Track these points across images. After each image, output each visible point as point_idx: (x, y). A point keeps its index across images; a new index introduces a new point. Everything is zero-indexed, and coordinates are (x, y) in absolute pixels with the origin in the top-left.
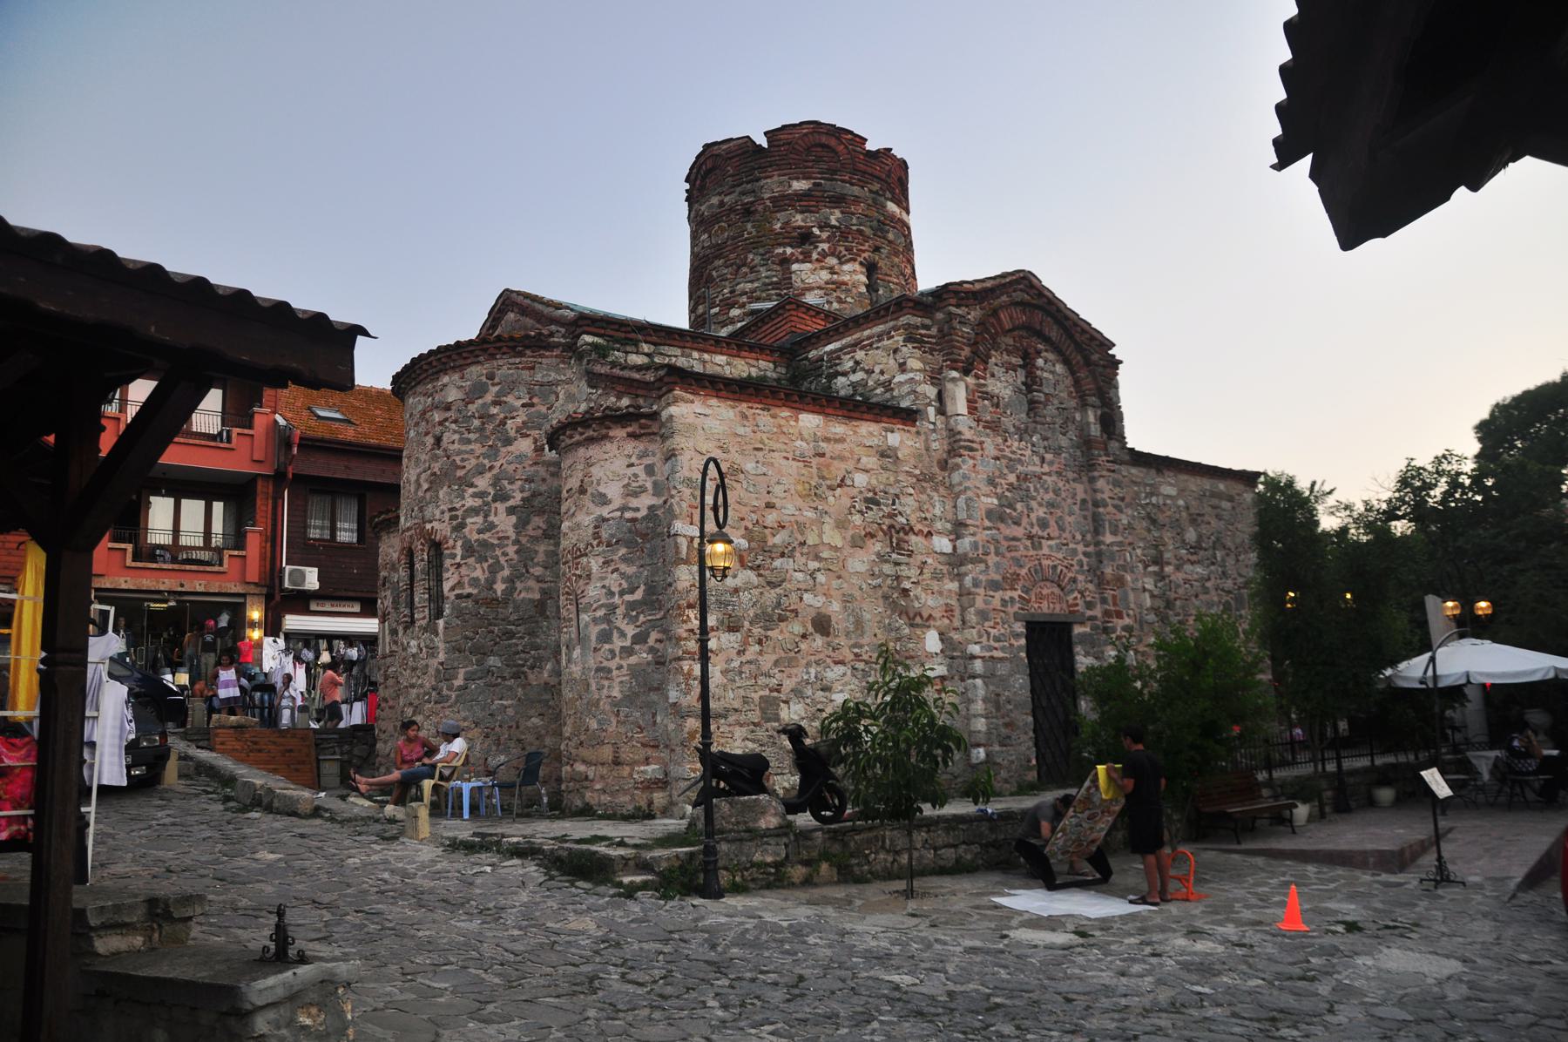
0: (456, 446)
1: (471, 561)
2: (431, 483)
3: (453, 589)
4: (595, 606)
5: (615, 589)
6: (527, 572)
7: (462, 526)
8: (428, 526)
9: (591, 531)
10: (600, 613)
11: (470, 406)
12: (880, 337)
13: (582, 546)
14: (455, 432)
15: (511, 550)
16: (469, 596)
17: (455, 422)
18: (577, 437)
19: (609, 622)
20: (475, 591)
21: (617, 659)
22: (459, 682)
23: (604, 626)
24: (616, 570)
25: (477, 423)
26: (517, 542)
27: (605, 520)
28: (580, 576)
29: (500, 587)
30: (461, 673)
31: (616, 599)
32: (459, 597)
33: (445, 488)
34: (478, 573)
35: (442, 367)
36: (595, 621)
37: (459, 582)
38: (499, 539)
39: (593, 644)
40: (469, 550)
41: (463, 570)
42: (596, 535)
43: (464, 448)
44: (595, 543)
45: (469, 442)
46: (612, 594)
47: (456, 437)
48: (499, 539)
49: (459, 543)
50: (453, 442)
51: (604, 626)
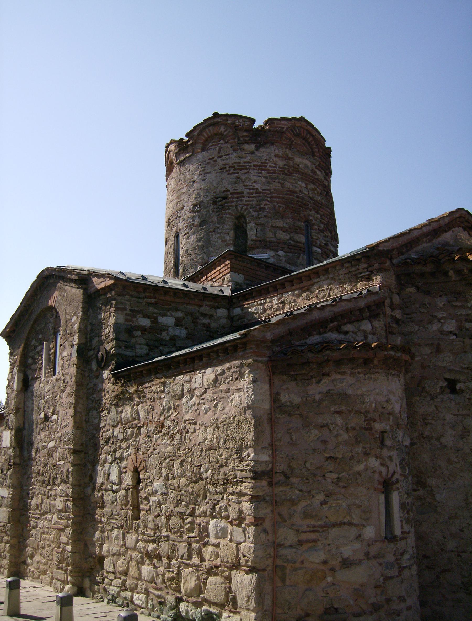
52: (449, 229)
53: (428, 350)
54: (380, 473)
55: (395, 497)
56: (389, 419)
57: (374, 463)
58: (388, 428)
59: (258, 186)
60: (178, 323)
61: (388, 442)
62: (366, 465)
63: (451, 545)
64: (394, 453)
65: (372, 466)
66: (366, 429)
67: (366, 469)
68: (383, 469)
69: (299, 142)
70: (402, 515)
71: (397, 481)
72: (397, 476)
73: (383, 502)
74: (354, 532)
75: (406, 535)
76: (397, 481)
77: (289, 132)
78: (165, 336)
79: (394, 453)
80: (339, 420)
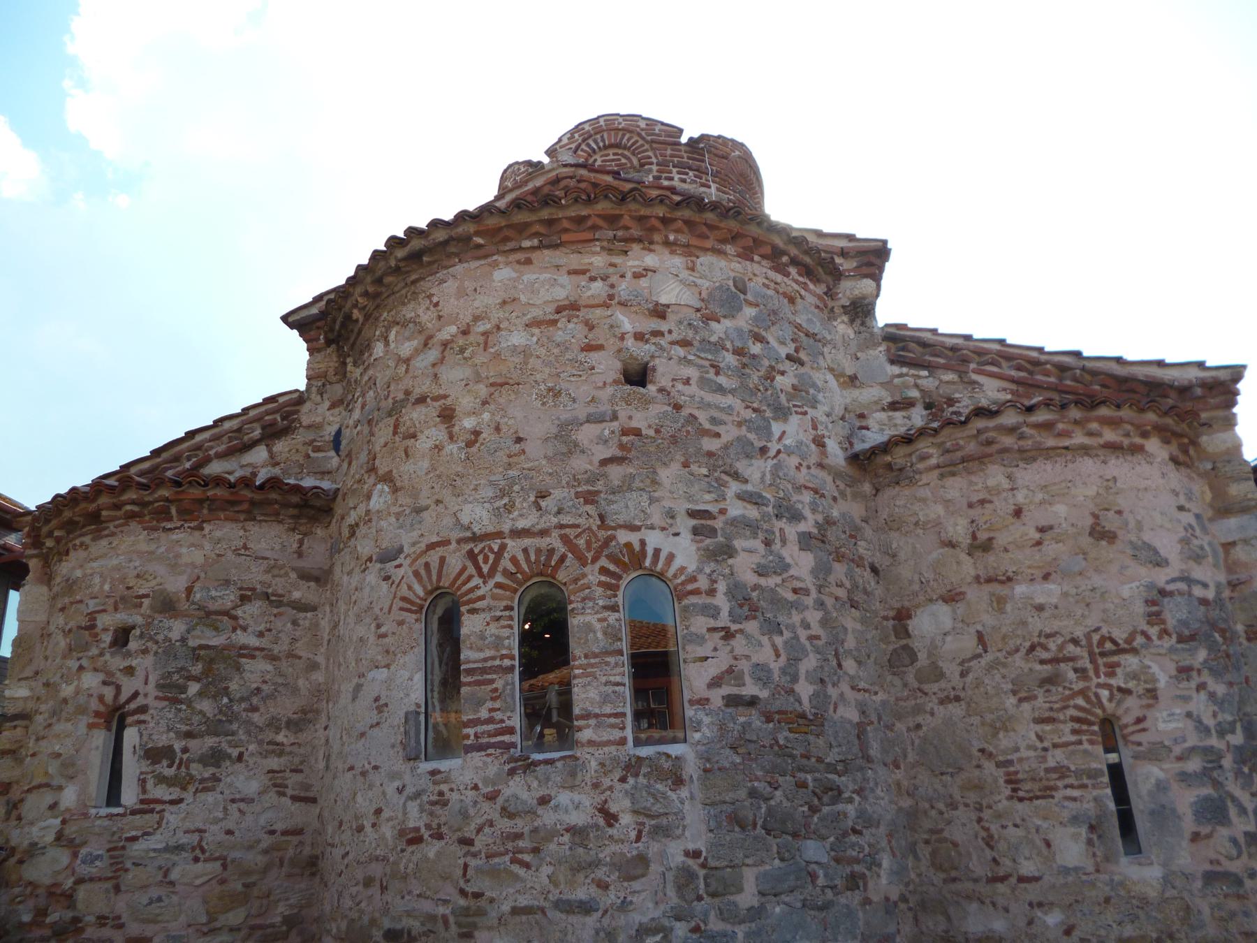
0: (693, 389)
1: (752, 627)
2: (622, 446)
3: (715, 683)
4: (1177, 750)
5: (1209, 721)
6: (840, 666)
7: (727, 551)
8: (623, 537)
9: (1139, 608)
10: (1194, 765)
11: (713, 324)
13: (1120, 635)
14: (684, 361)
15: (814, 617)
16: (753, 702)
17: (685, 343)
18: (1079, 439)
19: (1217, 784)
20: (764, 694)
21: (1245, 856)
22: (747, 898)
23: (1208, 791)
24: (1201, 687)
25: (730, 359)
26: (821, 605)
27: (1163, 593)
28: (1126, 692)
29: (805, 690)
30: (749, 878)
31: (1214, 741)
32: (733, 701)
33: (675, 467)
34: (765, 655)
35: (635, 232)
36: (1184, 777)
37: (730, 671)
38: (795, 591)
39: (1189, 824)
40: (746, 604)
41: (739, 644)
42: (1155, 617)
43: (710, 398)
44: (1153, 631)
45: (721, 390)
46: (1207, 730)
47: (692, 372)
48: (795, 591)
49: (721, 587)
50: (687, 382)
51: (1208, 791)
54: (101, 698)
55: (131, 736)
56: (141, 605)
58: (139, 620)
61: (133, 645)
62: (77, 686)
64: (143, 663)
65: (86, 686)
66: (86, 628)
67: (77, 693)
69: (611, 157)
70: (144, 769)
71: (143, 709)
72: (140, 701)
73: (97, 748)
75: (158, 807)
76: (143, 709)
77: (582, 150)
79: (143, 663)
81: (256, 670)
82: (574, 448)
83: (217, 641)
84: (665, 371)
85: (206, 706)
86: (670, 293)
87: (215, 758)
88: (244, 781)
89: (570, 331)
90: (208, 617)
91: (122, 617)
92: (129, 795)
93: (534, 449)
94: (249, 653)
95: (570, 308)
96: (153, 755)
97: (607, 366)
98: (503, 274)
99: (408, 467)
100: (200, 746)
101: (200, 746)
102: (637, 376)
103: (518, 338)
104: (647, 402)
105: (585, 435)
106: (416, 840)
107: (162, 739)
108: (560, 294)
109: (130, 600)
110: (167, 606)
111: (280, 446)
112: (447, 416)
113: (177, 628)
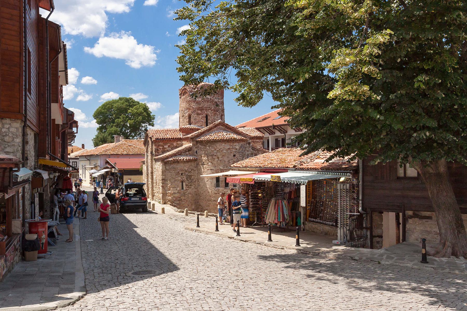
12: (257, 142)
52: (215, 127)
53: (200, 157)
55: (184, 184)
57: (179, 178)
59: (194, 107)
60: (169, 146)
61: (183, 175)
63: (202, 192)
64: (185, 177)
68: (182, 179)
74: (175, 189)
78: (166, 150)
79: (185, 177)
80: (174, 171)
81: (193, 177)
82: (230, 162)
83: (190, 174)
84: (237, 155)
85: (190, 181)
86: (237, 147)
87: (191, 185)
88: (193, 187)
89: (229, 151)
90: (190, 172)
91: (182, 172)
92: (185, 189)
93: (226, 162)
94: (192, 175)
95: (229, 149)
96: (186, 185)
97: (232, 155)
98: (223, 144)
99: (214, 162)
100: (190, 184)
101: (190, 184)
102: (234, 156)
103: (225, 151)
104: (235, 158)
105: (231, 161)
106: (216, 194)
107: (187, 184)
108: (228, 147)
109: (182, 170)
110: (186, 171)
111: (190, 152)
112: (218, 158)
113: (187, 173)
